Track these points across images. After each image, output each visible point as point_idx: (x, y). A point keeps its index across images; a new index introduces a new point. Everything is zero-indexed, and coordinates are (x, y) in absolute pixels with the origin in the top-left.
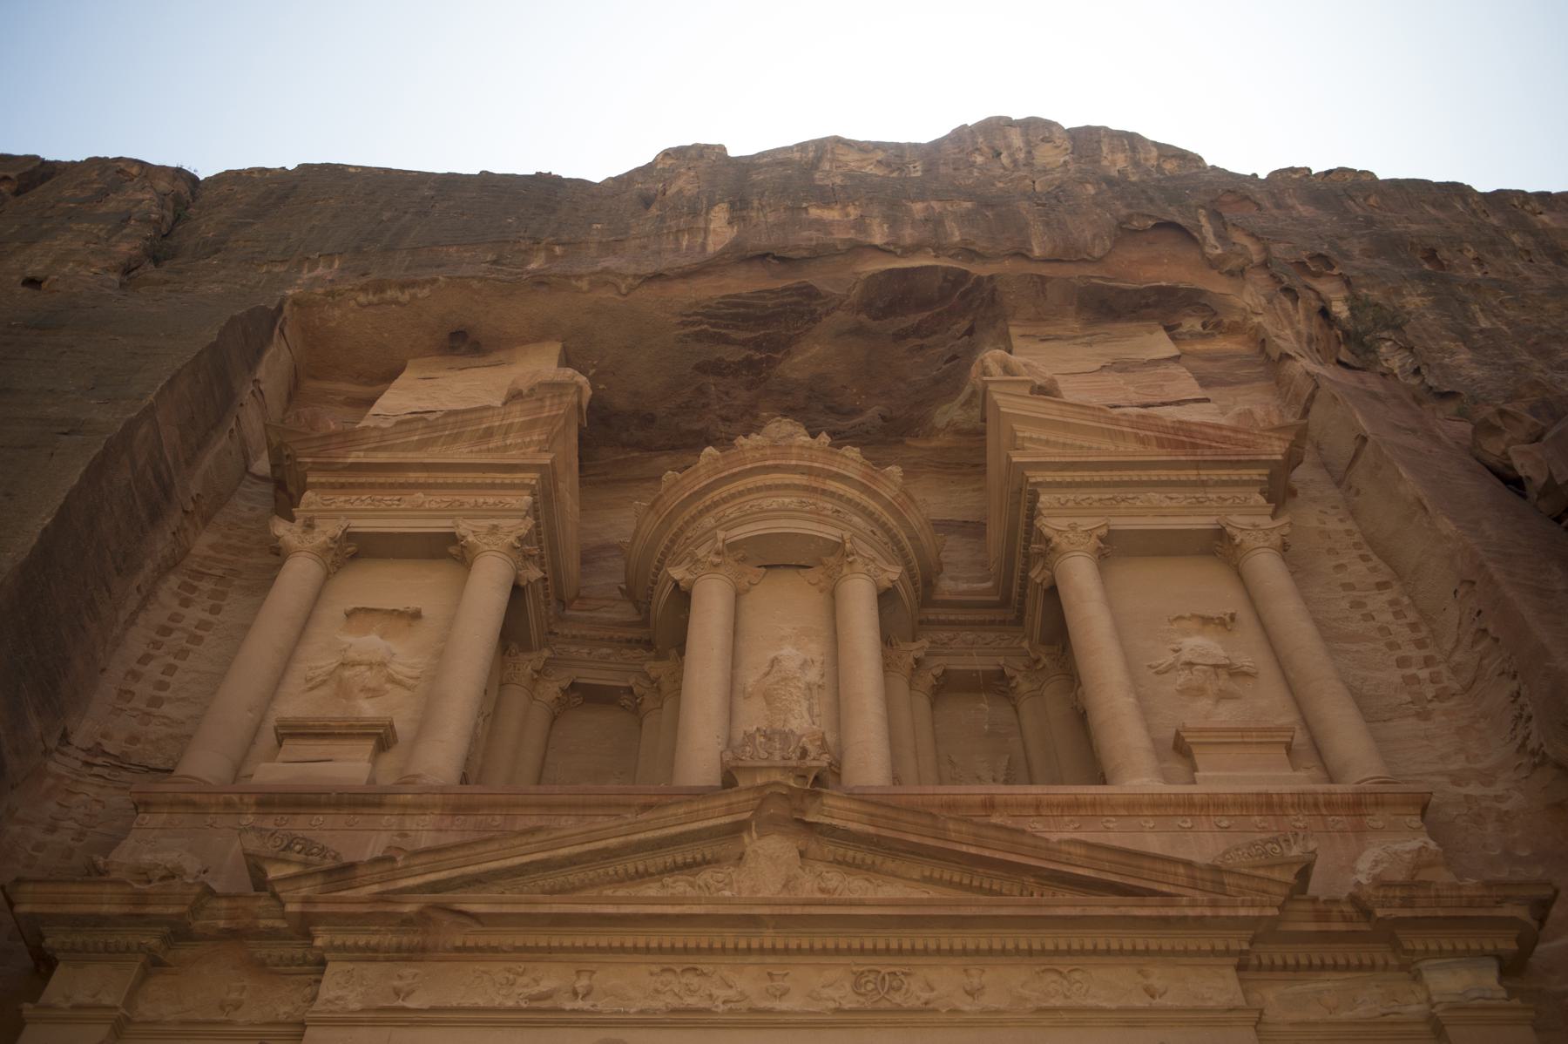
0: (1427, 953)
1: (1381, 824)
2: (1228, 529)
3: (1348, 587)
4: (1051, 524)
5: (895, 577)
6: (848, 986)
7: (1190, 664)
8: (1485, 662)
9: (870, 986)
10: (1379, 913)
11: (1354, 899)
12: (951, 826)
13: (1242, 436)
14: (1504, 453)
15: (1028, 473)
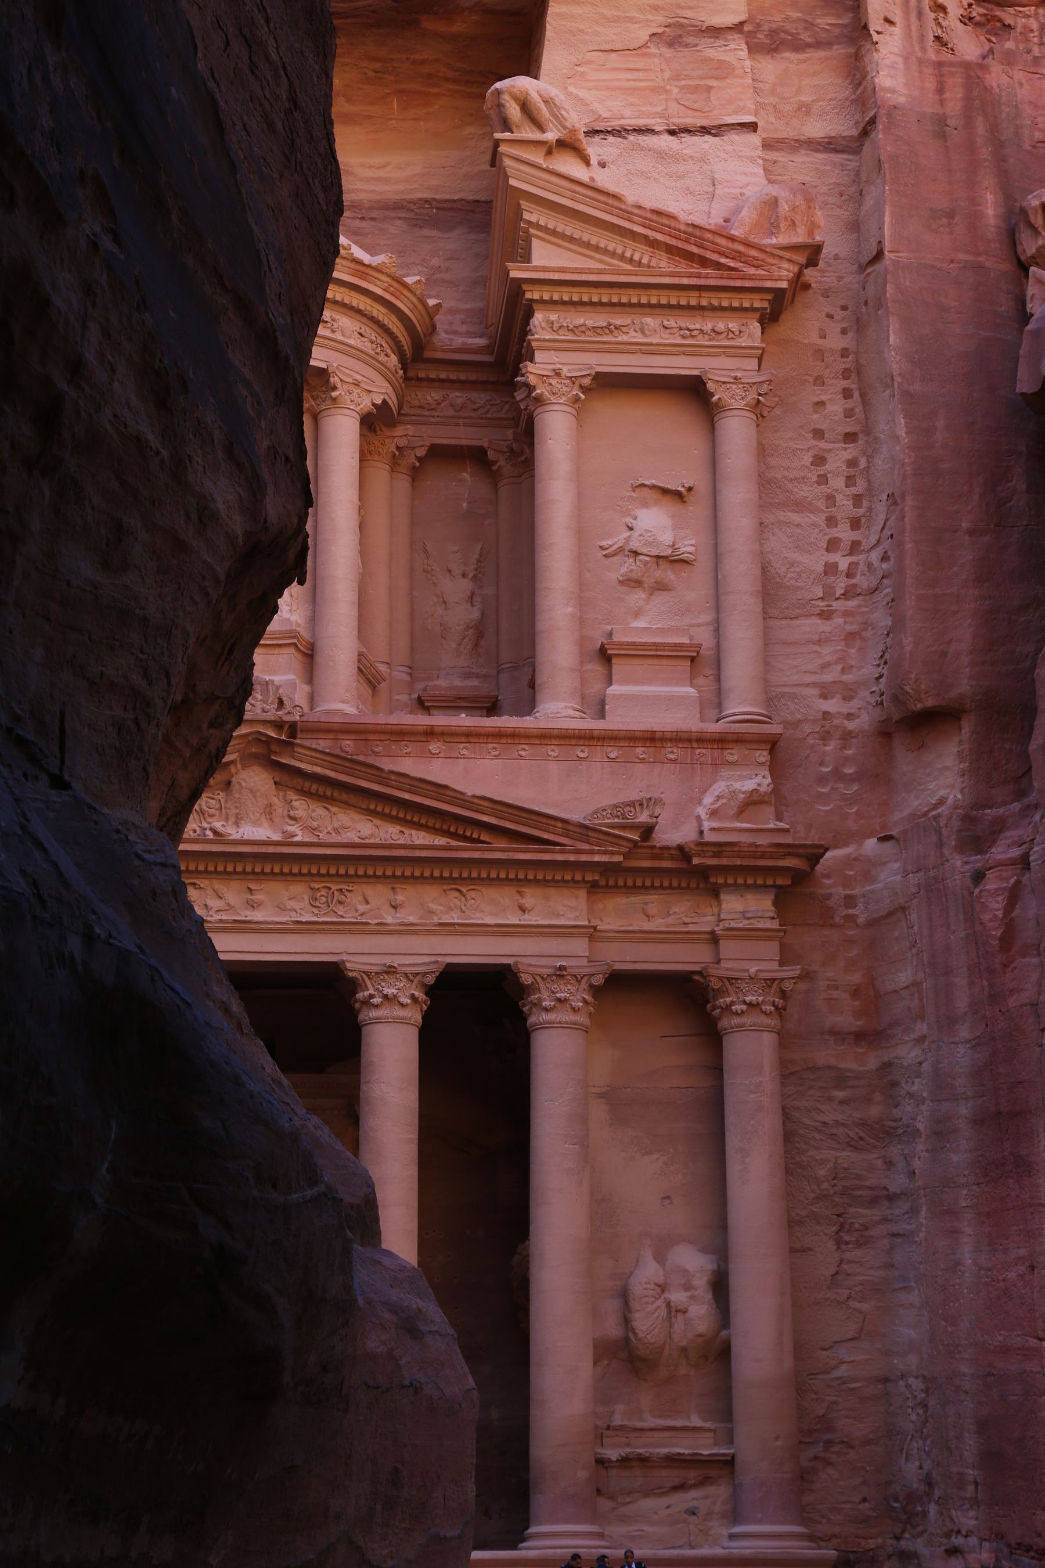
0: (726, 885)
1: (735, 758)
2: (710, 386)
3: (818, 434)
4: (538, 369)
5: (379, 402)
6: (306, 898)
7: (636, 553)
8: (885, 581)
9: (324, 899)
10: (696, 861)
11: (680, 848)
12: (393, 777)
13: (754, 253)
14: (1034, 260)
15: (525, 287)
